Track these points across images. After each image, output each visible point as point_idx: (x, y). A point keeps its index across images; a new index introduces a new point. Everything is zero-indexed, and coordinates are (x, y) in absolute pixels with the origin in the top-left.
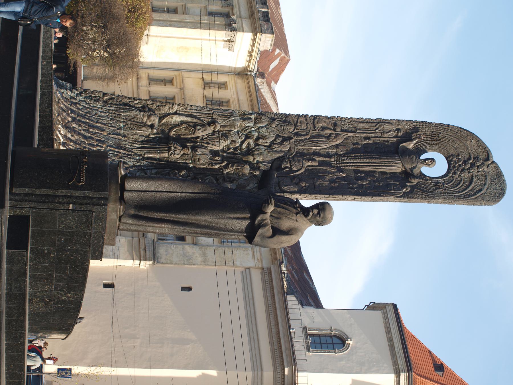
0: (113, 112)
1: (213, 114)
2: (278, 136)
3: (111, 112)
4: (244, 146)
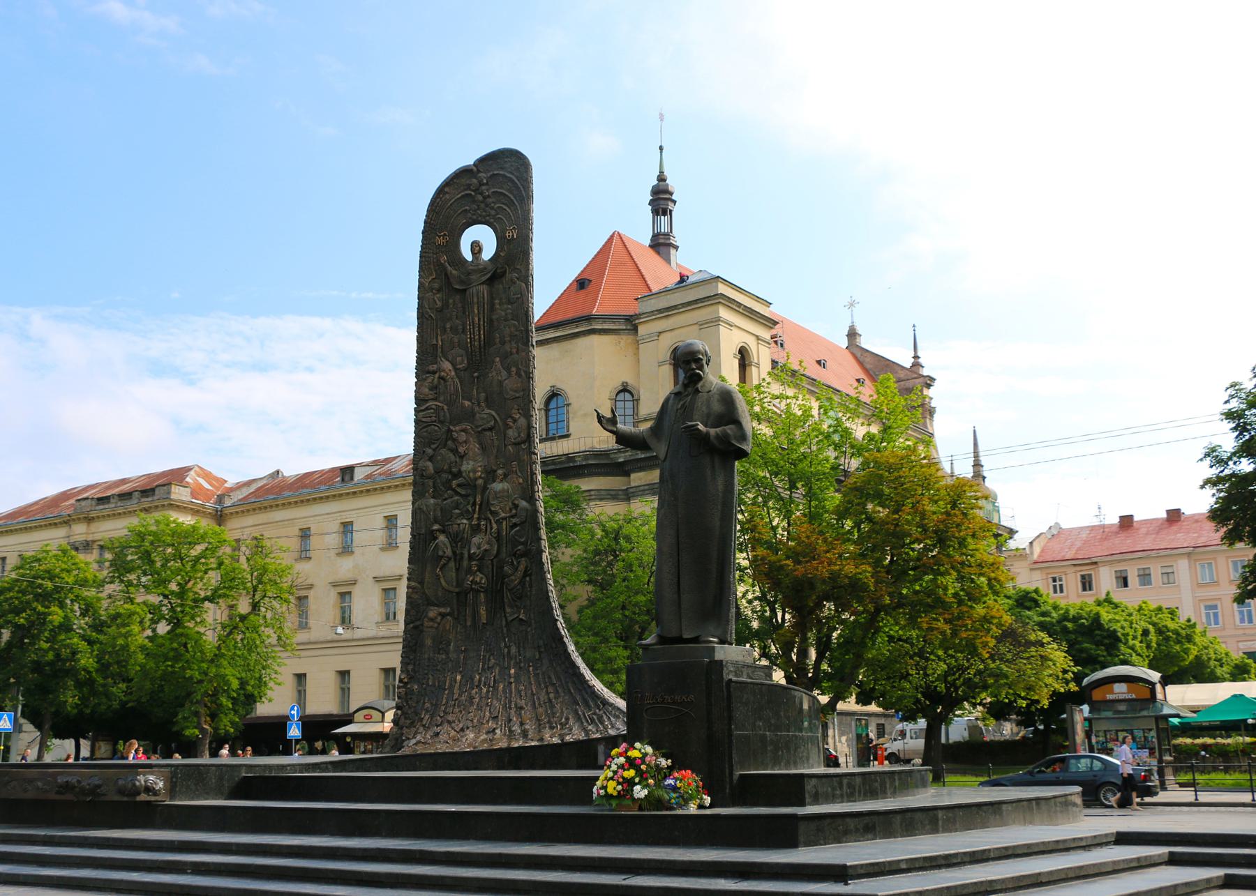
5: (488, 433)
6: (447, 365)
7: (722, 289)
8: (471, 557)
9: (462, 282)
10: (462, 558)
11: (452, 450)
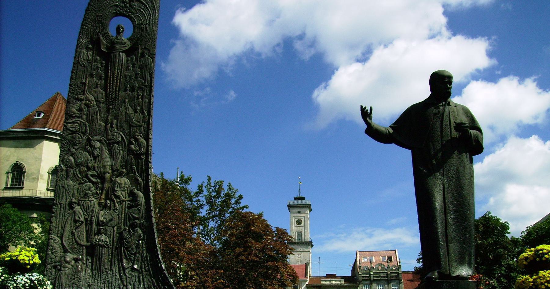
1: (61, 204)
2: (86, 150)
4: (93, 179)
6: (91, 97)
8: (99, 224)
9: (107, 48)
10: (91, 224)
11: (89, 152)
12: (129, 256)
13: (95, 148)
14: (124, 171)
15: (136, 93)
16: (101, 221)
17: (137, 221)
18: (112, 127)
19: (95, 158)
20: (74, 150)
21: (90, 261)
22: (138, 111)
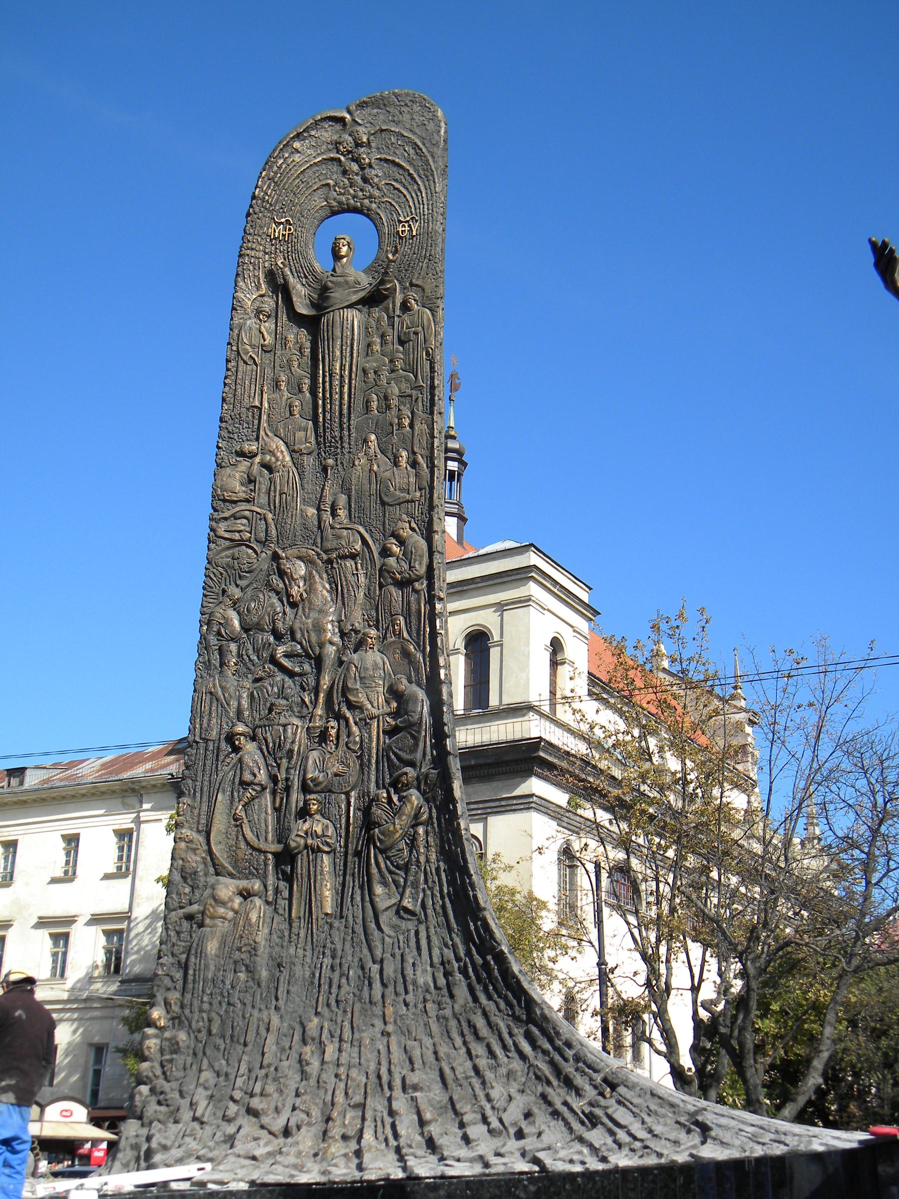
0: (205, 999)
2: (269, 586)
3: (206, 1006)
5: (349, 563)
7: (534, 559)
9: (313, 305)
10: (288, 789)
12: (391, 872)
13: (294, 580)
14: (373, 632)
15: (394, 411)
16: (313, 780)
17: (408, 769)
18: (334, 514)
19: (294, 605)
20: (237, 593)
21: (286, 894)
22: (403, 462)
